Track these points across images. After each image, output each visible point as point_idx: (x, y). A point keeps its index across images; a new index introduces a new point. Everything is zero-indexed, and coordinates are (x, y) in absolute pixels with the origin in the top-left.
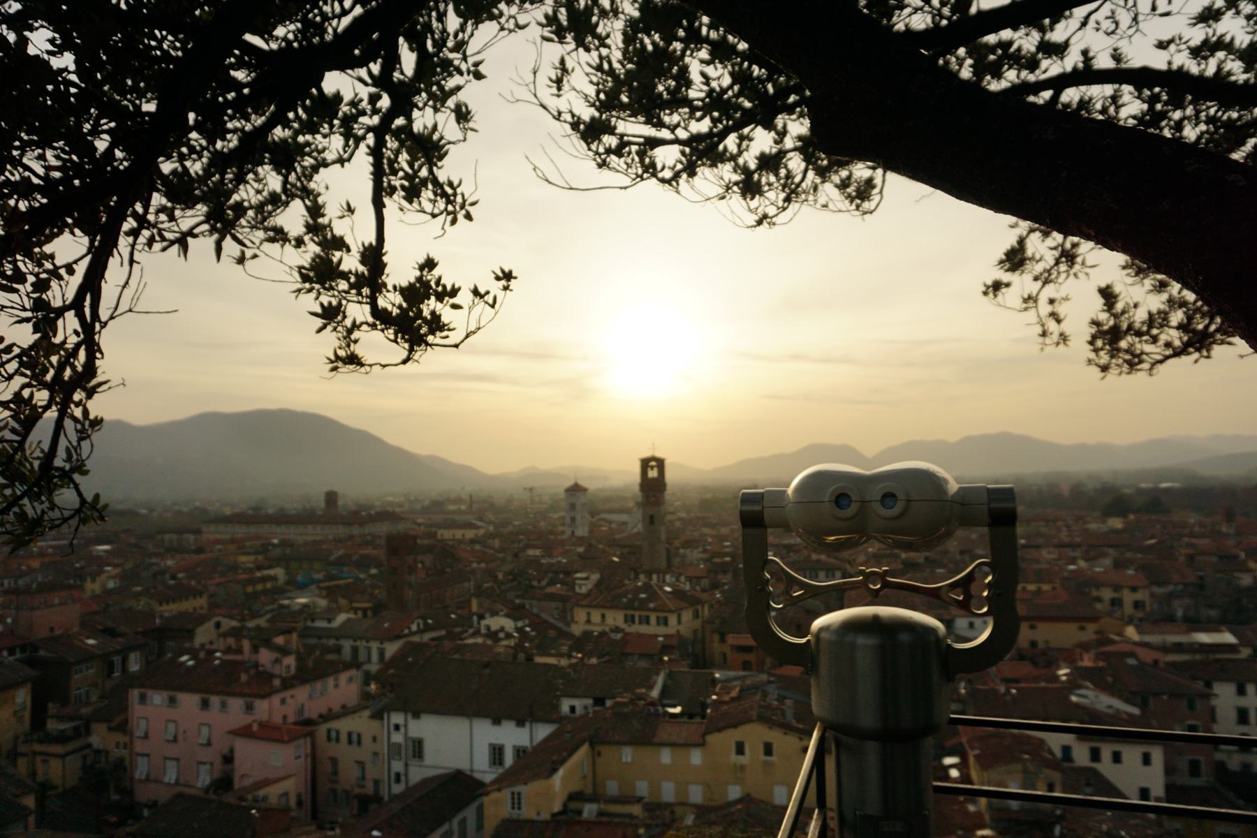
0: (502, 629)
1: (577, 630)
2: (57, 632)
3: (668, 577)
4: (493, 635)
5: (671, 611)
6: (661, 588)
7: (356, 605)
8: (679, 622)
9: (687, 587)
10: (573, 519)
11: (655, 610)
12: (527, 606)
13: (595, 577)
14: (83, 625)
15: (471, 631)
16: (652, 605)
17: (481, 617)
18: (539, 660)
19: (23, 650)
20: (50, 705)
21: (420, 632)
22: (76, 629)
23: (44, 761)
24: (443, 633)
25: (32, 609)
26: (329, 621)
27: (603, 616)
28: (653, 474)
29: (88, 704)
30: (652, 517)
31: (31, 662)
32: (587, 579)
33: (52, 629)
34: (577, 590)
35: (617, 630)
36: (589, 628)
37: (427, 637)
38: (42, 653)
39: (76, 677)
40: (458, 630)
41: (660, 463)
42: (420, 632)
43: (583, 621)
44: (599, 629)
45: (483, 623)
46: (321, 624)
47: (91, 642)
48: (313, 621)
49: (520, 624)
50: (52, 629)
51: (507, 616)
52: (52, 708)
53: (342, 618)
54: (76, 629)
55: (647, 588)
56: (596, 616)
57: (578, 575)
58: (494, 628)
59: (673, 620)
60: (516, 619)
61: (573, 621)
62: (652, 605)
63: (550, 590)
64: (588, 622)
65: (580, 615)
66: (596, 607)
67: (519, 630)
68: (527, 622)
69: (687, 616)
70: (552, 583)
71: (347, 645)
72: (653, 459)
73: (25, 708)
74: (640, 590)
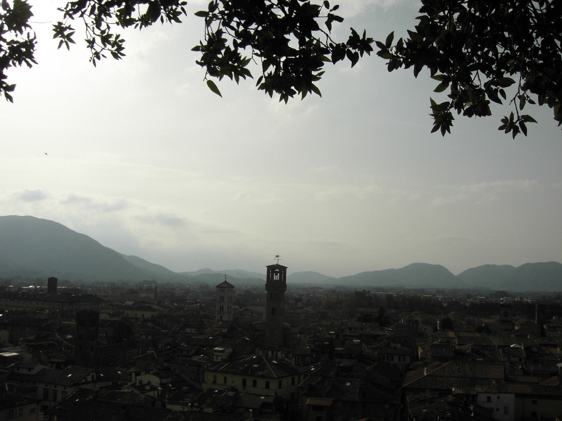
0: (149, 383)
1: (205, 387)
3: (279, 354)
4: (141, 387)
5: (274, 378)
6: (270, 361)
7: (52, 360)
8: (280, 387)
9: (293, 363)
10: (222, 308)
11: (262, 376)
12: (172, 369)
13: (230, 350)
15: (129, 384)
16: (260, 373)
17: (138, 374)
18: (169, 406)
21: (93, 381)
24: (110, 383)
26: (30, 370)
27: (225, 378)
28: (276, 277)
30: (273, 310)
32: (221, 351)
34: (215, 360)
35: (233, 389)
36: (214, 387)
37: (99, 385)
40: (120, 382)
41: (282, 270)
42: (93, 381)
43: (212, 381)
44: (222, 388)
45: (139, 378)
46: (25, 372)
48: (18, 369)
49: (164, 381)
51: (156, 374)
53: (38, 368)
55: (259, 360)
56: (220, 379)
57: (216, 348)
58: (145, 382)
59: (274, 385)
60: (161, 377)
61: (203, 380)
62: (260, 373)
63: (196, 358)
64: (214, 382)
65: (209, 377)
66: (221, 372)
67: (162, 385)
68: (170, 380)
69: (287, 382)
70: (198, 353)
71: (41, 388)
72: (277, 266)
74: (253, 361)
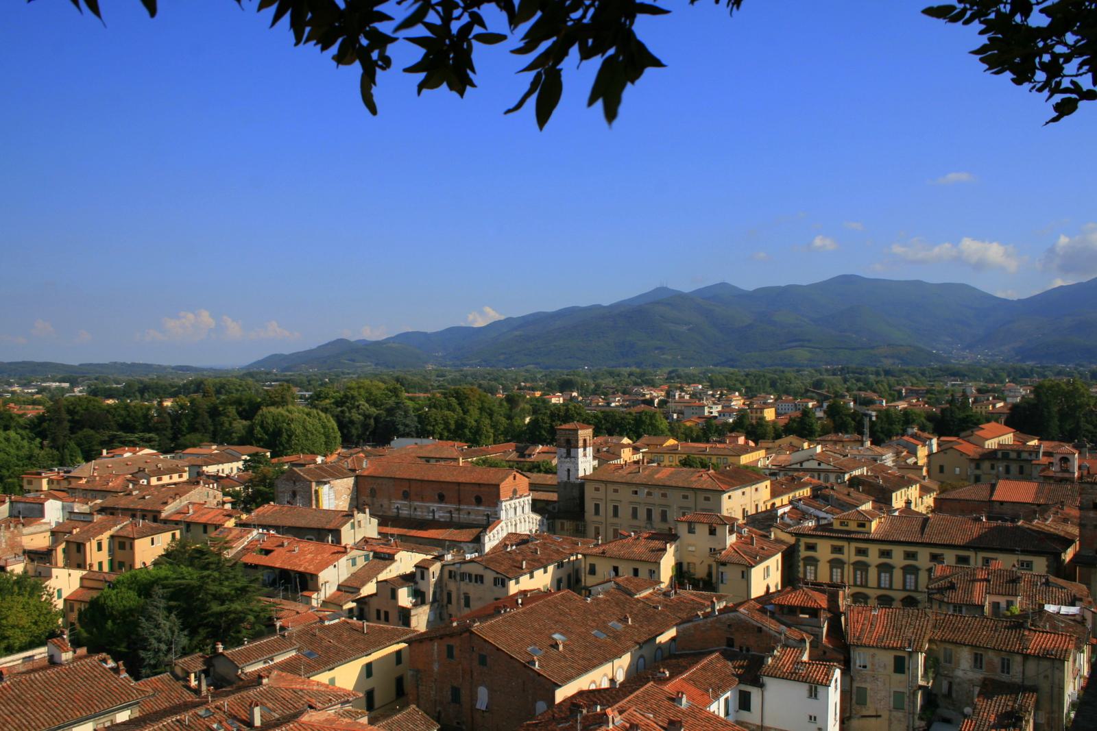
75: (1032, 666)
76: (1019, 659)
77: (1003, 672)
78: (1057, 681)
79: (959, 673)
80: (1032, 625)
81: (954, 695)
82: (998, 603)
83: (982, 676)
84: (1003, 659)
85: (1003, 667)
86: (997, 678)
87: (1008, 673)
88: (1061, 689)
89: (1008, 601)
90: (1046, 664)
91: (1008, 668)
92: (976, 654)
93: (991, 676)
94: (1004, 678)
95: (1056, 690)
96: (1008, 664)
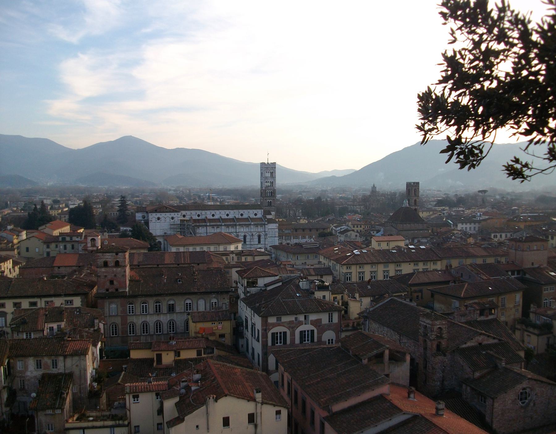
2: (536, 266)
14: (549, 263)
19: (518, 274)
20: (532, 305)
22: (545, 265)
23: (528, 335)
25: (523, 251)
29: (551, 309)
31: (523, 280)
33: (533, 264)
38: (527, 276)
39: (544, 292)
47: (553, 274)
50: (533, 264)
52: (533, 308)
54: (545, 265)
73: (519, 305)
75: (69, 361)
76: (61, 358)
77: (53, 368)
78: (82, 367)
79: (28, 374)
80: (69, 337)
81: (26, 387)
82: (53, 327)
83: (42, 372)
84: (53, 360)
85: (53, 365)
86: (50, 372)
87: (56, 368)
88: (85, 370)
89: (58, 325)
90: (76, 358)
91: (56, 365)
92: (37, 361)
93: (48, 372)
94: (55, 371)
95: (82, 371)
96: (56, 363)
